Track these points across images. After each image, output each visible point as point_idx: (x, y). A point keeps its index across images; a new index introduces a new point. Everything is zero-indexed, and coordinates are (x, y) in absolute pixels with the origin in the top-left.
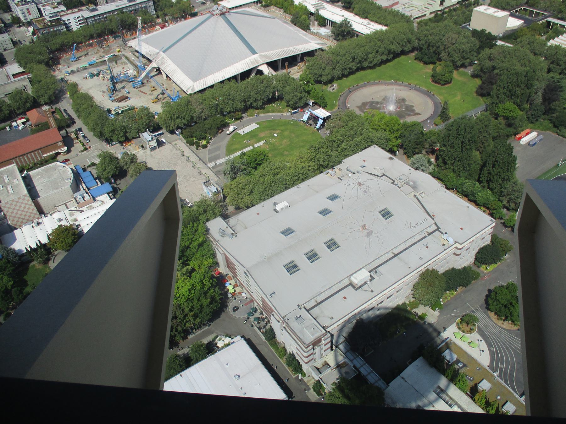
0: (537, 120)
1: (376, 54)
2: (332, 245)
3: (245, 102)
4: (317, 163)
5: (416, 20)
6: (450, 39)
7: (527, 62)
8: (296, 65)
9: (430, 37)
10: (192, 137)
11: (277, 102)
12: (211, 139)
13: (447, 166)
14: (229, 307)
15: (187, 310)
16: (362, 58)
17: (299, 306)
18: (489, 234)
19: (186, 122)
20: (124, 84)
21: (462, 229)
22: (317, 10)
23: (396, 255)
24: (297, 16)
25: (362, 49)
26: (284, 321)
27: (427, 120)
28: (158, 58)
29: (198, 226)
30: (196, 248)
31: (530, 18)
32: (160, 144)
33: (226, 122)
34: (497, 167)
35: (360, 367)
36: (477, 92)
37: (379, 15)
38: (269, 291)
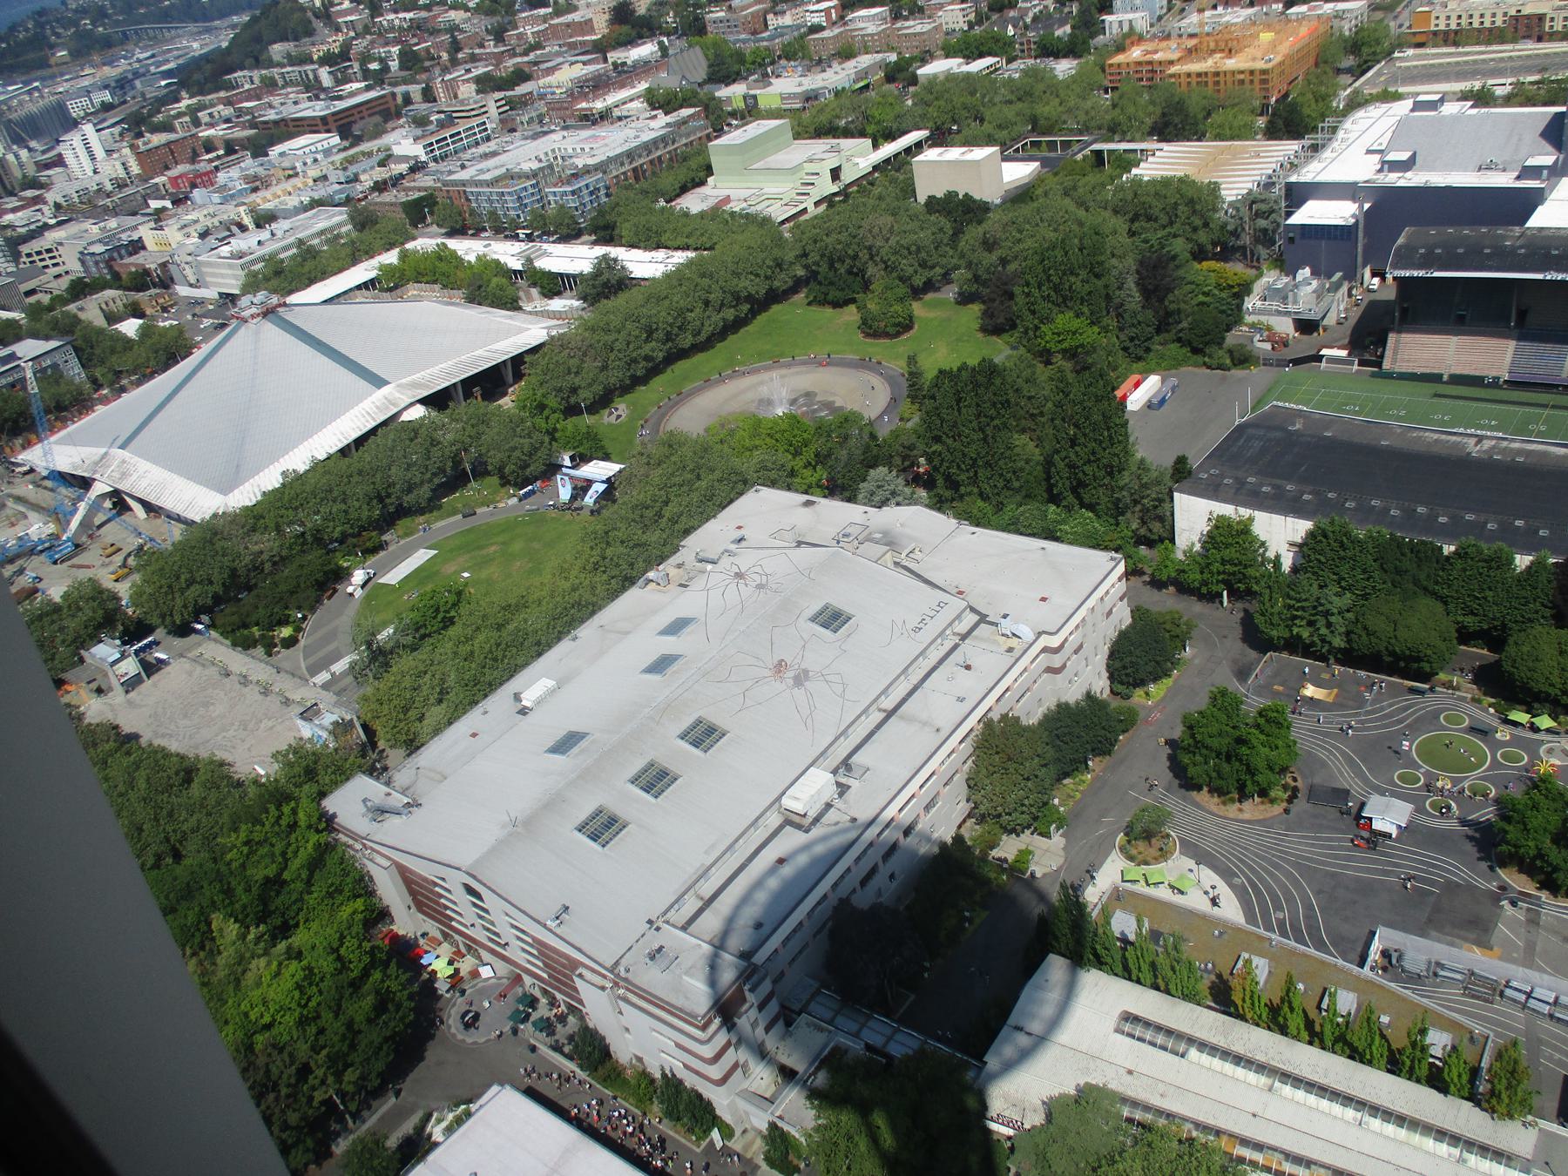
0: (1148, 350)
1: (705, 311)
2: (703, 735)
3: (381, 499)
4: (613, 574)
5: (787, 225)
6: (876, 230)
7: (1074, 227)
8: (505, 394)
9: (829, 240)
10: (246, 626)
11: (473, 484)
12: (304, 618)
13: (963, 490)
14: (451, 1022)
15: (303, 1050)
16: (671, 325)
17: (650, 922)
18: (1121, 599)
19: (218, 588)
20: (20, 562)
21: (1044, 599)
22: (529, 261)
23: (890, 714)
24: (478, 283)
25: (667, 302)
26: (620, 982)
27: (881, 416)
28: (109, 466)
29: (294, 812)
30: (304, 876)
31: (1052, 155)
32: (151, 668)
33: (340, 568)
34: (1082, 440)
35: (887, 1042)
36: (984, 330)
37: (687, 230)
38: (546, 912)
